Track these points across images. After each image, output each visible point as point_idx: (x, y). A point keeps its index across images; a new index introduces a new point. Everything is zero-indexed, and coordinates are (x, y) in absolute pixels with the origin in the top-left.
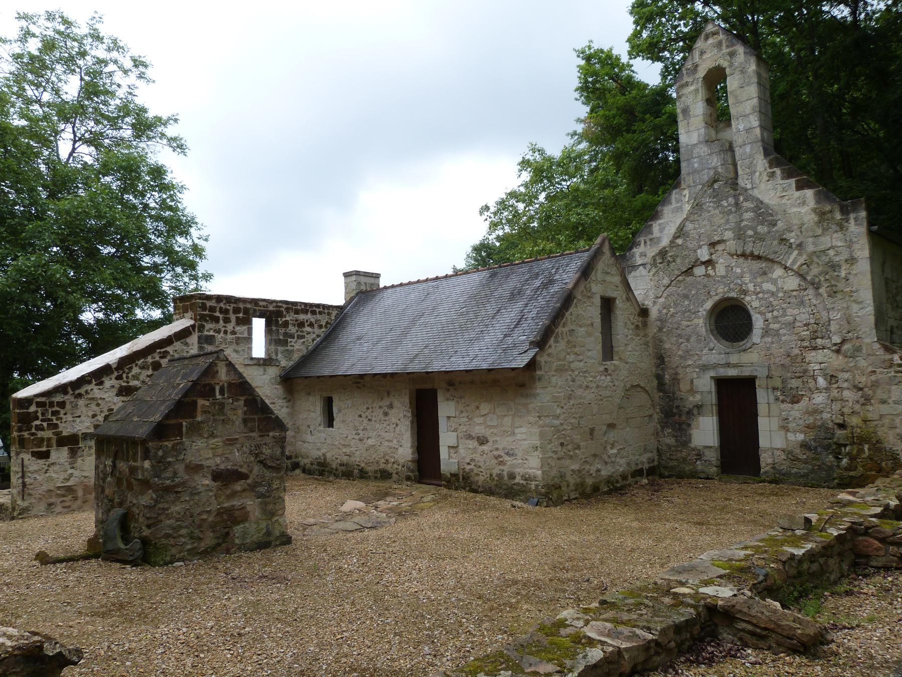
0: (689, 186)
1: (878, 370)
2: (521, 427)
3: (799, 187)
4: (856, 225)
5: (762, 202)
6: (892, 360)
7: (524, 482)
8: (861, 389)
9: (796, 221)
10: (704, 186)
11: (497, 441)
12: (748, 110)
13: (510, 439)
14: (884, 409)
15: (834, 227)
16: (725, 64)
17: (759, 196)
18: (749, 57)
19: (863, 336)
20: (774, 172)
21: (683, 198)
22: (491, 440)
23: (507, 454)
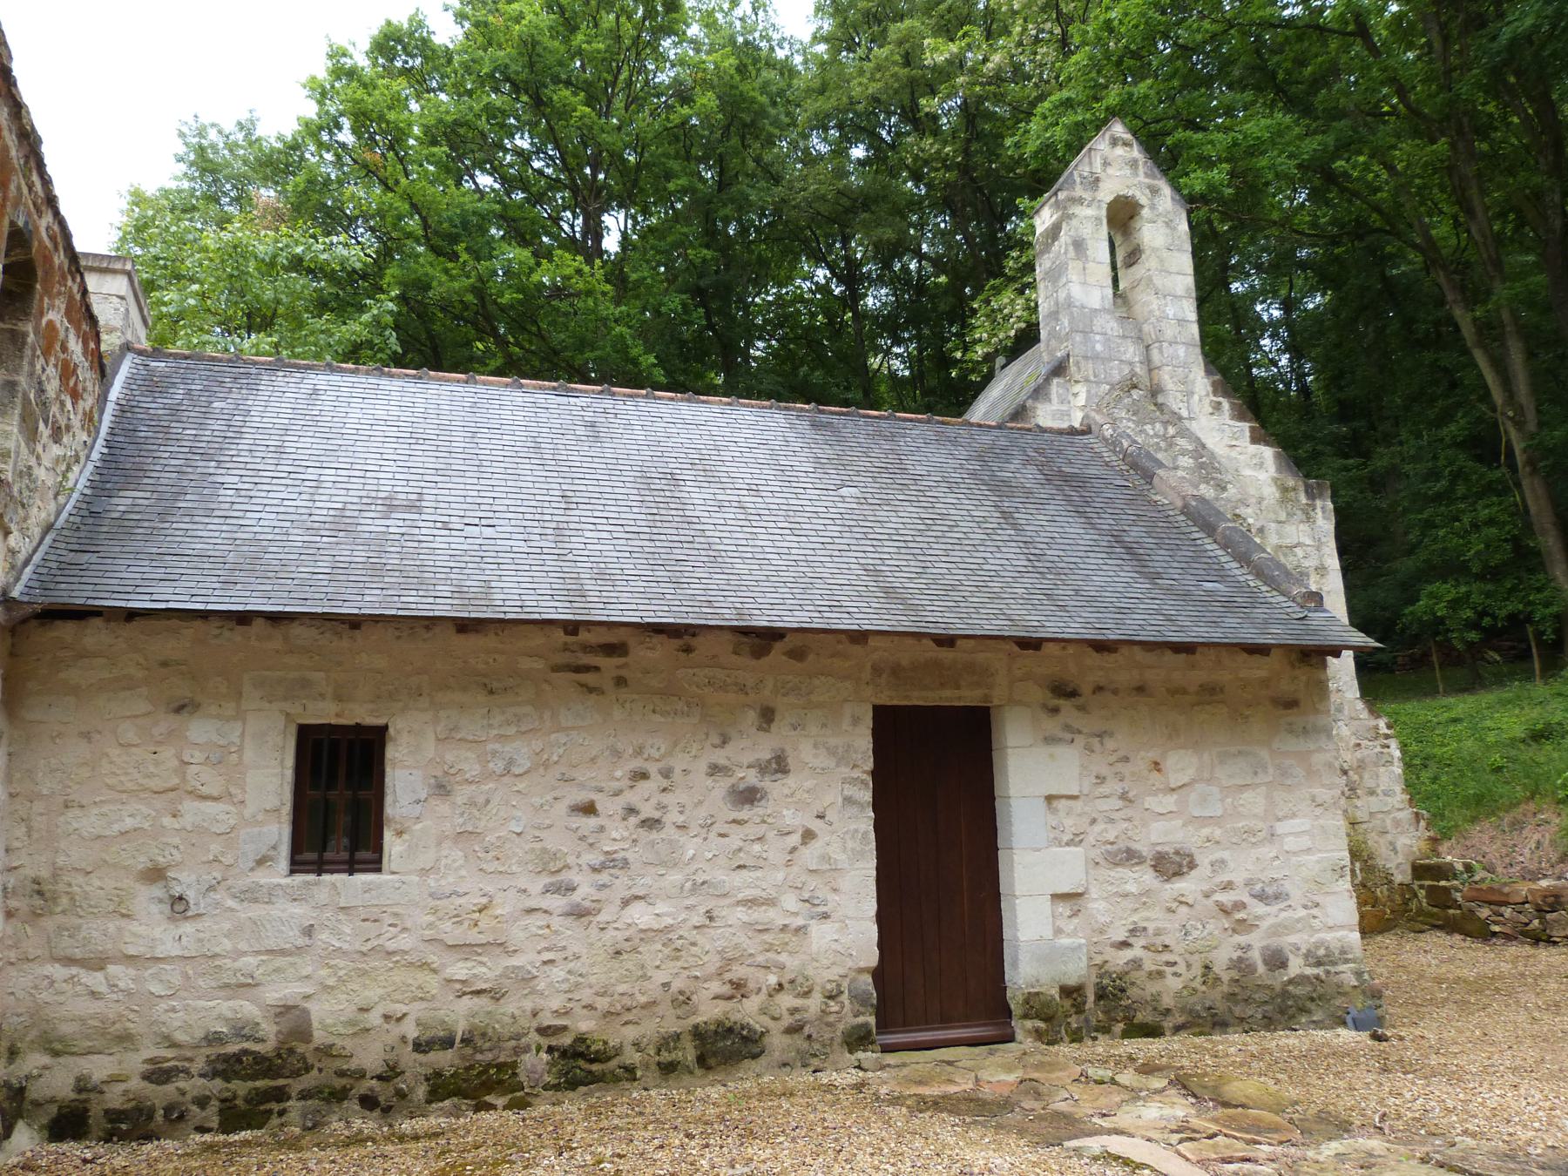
0: (1087, 380)
1: (1364, 743)
2: (1294, 816)
3: (1255, 440)
4: (1324, 518)
5: (1204, 446)
6: (1376, 727)
7: (1319, 971)
8: (1345, 773)
9: (1252, 491)
10: (1113, 387)
11: (1223, 862)
12: (1180, 291)
13: (1268, 851)
14: (1374, 803)
15: (1299, 513)
16: (1143, 200)
17: (1200, 435)
18: (1178, 207)
19: (1344, 689)
20: (1220, 403)
21: (1071, 398)
22: (1203, 860)
23: (1262, 897)
